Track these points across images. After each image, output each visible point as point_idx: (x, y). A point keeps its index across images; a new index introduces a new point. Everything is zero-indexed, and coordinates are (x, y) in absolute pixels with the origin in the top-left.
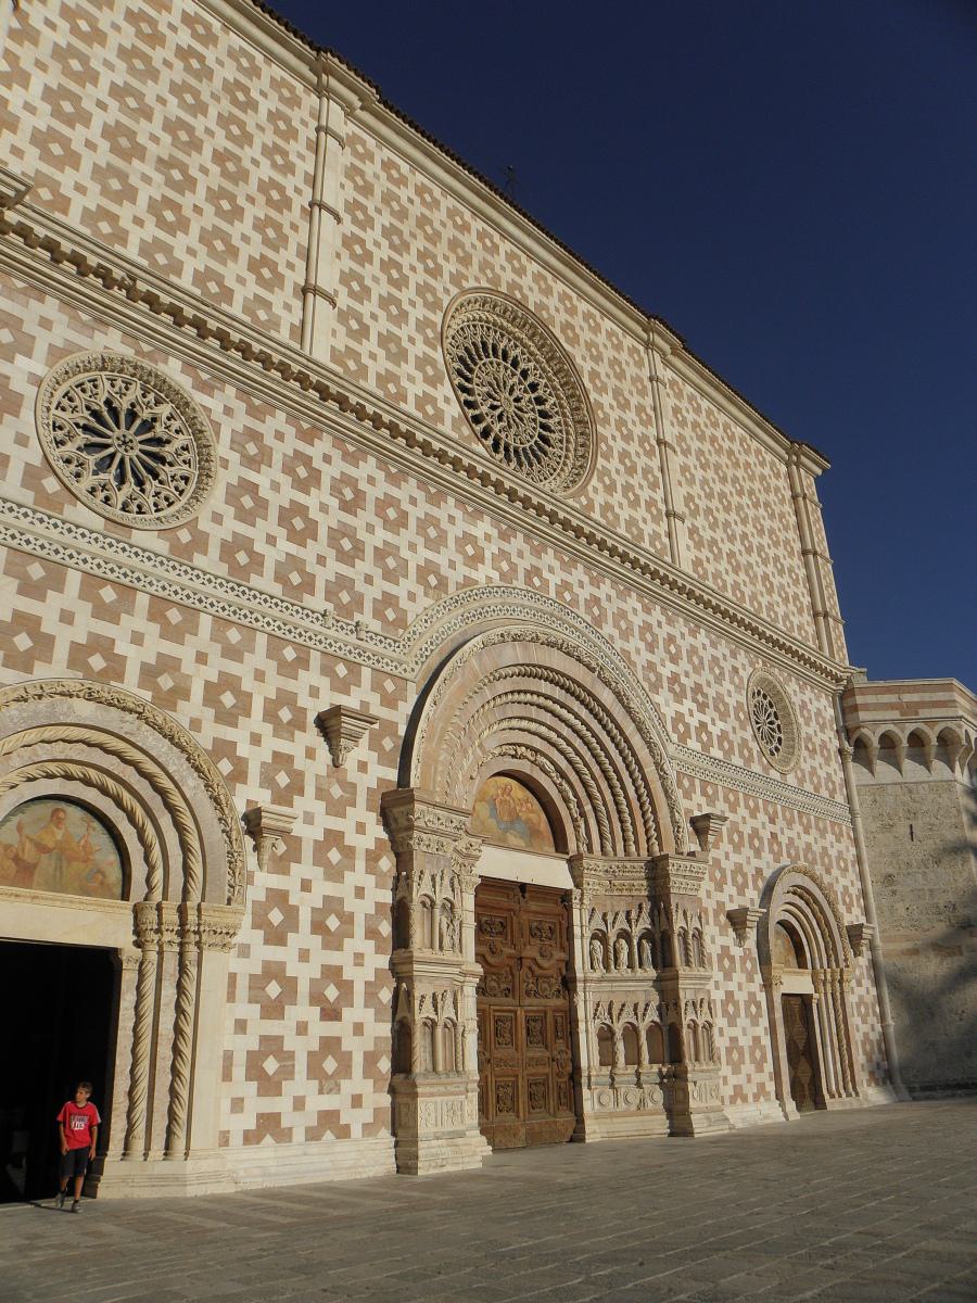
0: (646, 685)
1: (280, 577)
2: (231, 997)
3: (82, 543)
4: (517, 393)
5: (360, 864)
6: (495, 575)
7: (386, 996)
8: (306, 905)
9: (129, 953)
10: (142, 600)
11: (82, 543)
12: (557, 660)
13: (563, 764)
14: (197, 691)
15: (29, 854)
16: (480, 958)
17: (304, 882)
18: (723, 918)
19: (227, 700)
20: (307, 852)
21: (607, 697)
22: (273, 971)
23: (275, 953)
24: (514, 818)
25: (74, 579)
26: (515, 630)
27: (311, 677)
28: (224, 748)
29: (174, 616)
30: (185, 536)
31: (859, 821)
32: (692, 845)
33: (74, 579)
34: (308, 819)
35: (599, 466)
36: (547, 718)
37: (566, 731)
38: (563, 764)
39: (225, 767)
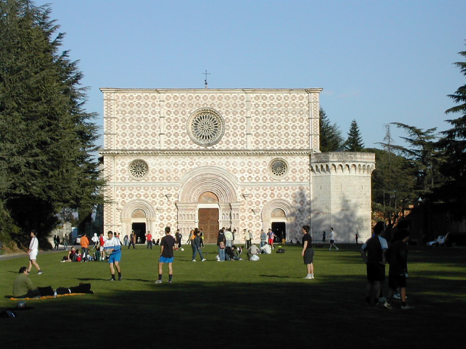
0: (233, 173)
1: (159, 179)
2: (156, 226)
3: (135, 184)
4: (209, 123)
5: (173, 211)
6: (196, 166)
7: (176, 225)
8: (165, 216)
9: (146, 223)
10: (142, 188)
11: (135, 184)
12: (209, 176)
13: (216, 189)
14: (150, 196)
15: (136, 214)
16: (199, 219)
17: (165, 214)
18: (250, 210)
19: (154, 196)
20: (165, 210)
21: (220, 179)
22: (161, 223)
23: (161, 222)
24: (210, 198)
25: (135, 188)
26: (199, 174)
27: (165, 190)
28: (154, 201)
29: (146, 188)
30: (146, 179)
31: (311, 185)
32: (243, 199)
33: (135, 188)
34: (165, 207)
35: (225, 133)
36: (211, 183)
37: (215, 185)
38: (216, 189)
39: (154, 203)
